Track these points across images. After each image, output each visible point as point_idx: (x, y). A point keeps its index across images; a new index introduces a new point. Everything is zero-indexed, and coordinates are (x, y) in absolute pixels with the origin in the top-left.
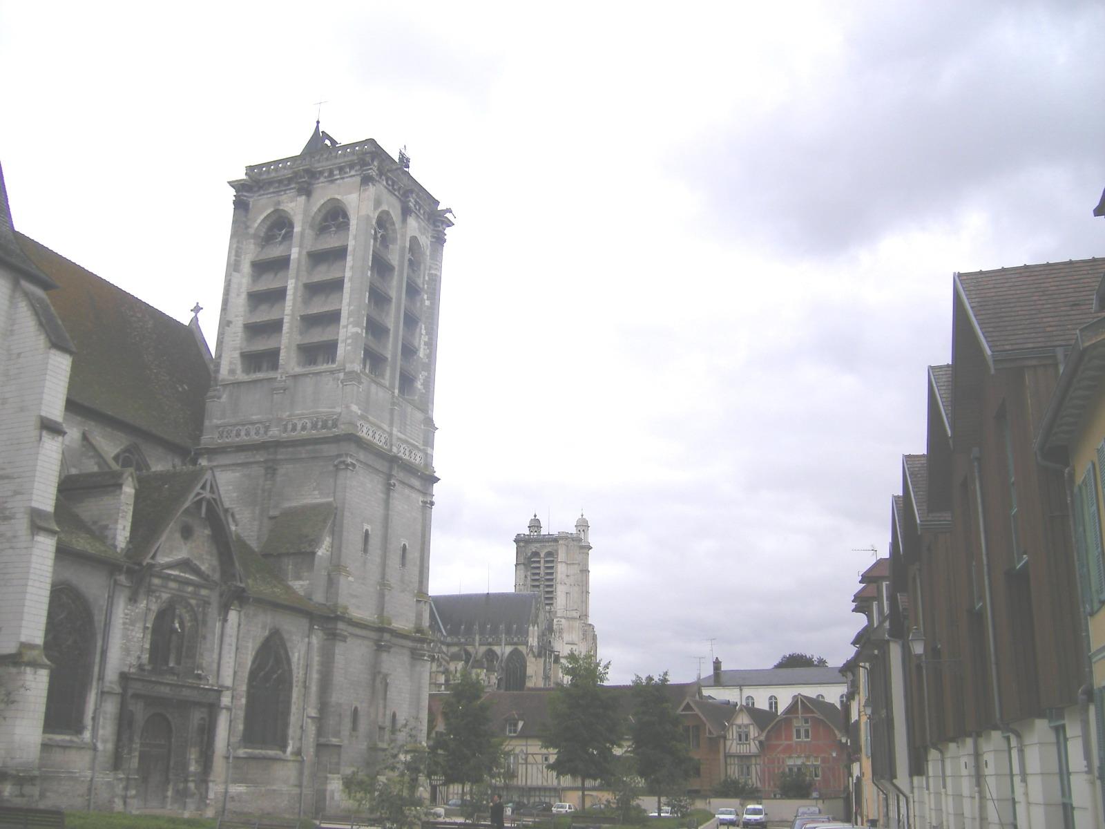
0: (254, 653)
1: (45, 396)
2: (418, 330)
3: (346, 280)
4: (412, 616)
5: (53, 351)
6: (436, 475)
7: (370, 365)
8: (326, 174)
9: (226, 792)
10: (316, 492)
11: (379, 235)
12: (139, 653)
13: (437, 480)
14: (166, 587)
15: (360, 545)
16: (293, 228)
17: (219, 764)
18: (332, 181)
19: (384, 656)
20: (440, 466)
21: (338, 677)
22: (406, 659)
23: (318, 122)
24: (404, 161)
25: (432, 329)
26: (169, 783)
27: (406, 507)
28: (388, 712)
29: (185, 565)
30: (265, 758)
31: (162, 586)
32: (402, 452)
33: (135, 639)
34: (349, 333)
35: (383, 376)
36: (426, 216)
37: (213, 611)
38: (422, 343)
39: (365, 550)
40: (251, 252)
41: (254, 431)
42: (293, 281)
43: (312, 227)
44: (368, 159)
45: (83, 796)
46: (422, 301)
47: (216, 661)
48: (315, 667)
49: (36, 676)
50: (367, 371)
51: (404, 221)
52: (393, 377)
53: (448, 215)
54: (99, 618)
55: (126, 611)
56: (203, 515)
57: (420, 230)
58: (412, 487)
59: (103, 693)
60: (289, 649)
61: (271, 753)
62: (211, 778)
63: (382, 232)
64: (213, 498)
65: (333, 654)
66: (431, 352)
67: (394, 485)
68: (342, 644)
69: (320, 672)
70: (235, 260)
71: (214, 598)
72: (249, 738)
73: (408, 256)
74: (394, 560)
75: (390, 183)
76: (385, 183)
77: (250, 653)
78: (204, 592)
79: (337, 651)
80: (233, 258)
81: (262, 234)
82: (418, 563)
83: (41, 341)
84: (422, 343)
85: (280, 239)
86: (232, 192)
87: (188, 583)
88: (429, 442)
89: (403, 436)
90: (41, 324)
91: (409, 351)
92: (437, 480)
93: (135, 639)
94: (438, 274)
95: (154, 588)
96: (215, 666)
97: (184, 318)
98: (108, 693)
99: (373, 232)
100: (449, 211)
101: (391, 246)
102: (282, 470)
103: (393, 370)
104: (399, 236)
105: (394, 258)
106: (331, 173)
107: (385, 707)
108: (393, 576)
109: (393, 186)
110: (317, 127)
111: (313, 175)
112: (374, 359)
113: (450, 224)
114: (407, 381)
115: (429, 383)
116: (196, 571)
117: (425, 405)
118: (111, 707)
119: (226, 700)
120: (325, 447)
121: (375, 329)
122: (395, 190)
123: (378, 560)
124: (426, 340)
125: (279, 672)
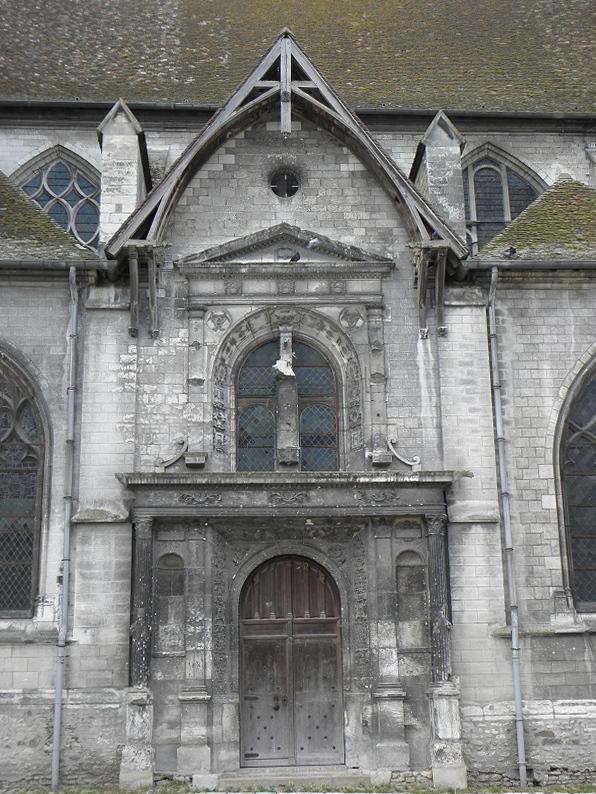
33: (166, 409)
45: (33, 743)
54: (49, 383)
55: (124, 358)
59: (73, 526)
64: (308, 91)
77: (547, 392)
93: (166, 409)
95: (200, 301)
96: (431, 433)
98: (76, 524)
118: (105, 553)
119: (474, 502)
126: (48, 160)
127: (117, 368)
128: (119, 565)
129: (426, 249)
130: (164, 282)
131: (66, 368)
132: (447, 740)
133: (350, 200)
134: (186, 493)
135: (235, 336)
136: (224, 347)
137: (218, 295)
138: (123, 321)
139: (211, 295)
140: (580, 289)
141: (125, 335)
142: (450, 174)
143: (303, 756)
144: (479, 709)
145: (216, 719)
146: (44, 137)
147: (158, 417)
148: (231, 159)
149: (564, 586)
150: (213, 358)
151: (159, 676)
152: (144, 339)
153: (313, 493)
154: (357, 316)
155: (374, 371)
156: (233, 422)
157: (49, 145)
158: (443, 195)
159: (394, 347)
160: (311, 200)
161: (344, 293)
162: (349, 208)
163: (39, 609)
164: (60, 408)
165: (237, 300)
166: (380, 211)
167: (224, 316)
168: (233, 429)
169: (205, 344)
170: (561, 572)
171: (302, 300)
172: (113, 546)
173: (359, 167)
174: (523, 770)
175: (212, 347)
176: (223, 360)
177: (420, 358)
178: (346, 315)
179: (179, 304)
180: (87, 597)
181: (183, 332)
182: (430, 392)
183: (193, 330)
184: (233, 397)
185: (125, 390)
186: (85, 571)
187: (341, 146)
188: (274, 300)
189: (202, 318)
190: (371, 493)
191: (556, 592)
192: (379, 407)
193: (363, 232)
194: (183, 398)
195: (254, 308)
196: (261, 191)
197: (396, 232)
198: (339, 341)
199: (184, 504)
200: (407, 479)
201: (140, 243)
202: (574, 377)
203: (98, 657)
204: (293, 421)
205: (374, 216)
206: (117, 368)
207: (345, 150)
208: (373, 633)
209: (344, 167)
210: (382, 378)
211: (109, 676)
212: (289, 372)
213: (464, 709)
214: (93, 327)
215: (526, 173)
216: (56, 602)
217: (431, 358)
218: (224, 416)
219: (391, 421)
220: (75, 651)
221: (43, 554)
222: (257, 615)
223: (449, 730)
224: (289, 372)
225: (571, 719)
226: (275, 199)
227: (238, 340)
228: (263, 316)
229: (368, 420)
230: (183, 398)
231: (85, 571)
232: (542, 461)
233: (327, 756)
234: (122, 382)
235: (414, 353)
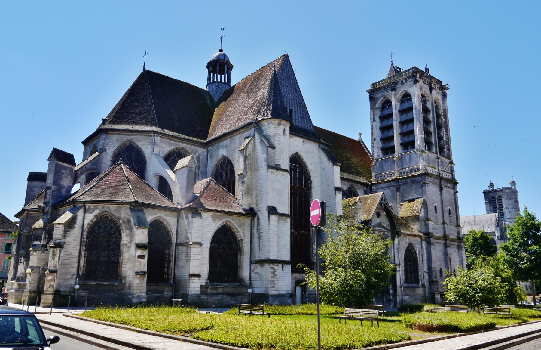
1: (335, 181)
2: (442, 131)
3: (414, 119)
4: (456, 234)
6: (457, 182)
7: (427, 146)
8: (400, 82)
9: (402, 299)
10: (416, 194)
11: (423, 100)
13: (458, 183)
15: (434, 211)
16: (392, 103)
17: (399, 289)
18: (403, 84)
19: (448, 249)
20: (458, 178)
21: (434, 258)
22: (456, 249)
23: (392, 61)
24: (427, 70)
25: (447, 129)
26: (384, 297)
27: (448, 195)
28: (452, 269)
29: (380, 225)
30: (413, 287)
32: (444, 175)
34: (419, 137)
35: (432, 149)
36: (439, 88)
38: (444, 135)
39: (436, 213)
40: (378, 113)
41: (390, 175)
42: (395, 122)
43: (398, 102)
44: (415, 74)
46: (442, 119)
47: (393, 256)
48: (425, 255)
50: (427, 149)
51: (431, 92)
52: (436, 150)
53: (447, 86)
56: (383, 209)
57: (437, 94)
58: (449, 187)
61: (414, 285)
62: (397, 295)
63: (424, 98)
65: (431, 250)
66: (448, 137)
67: (443, 188)
68: (433, 246)
69: (427, 257)
70: (373, 117)
72: (407, 281)
73: (434, 104)
74: (446, 214)
75: (424, 80)
76: (422, 81)
78: (386, 233)
79: (432, 249)
80: (372, 117)
81: (381, 107)
82: (455, 214)
83: (330, 164)
84: (444, 135)
85: (387, 107)
86: (368, 94)
87: (381, 231)
88: (452, 170)
89: (443, 170)
90: (329, 158)
91: (440, 138)
92: (458, 183)
94: (446, 108)
96: (393, 258)
97: (356, 138)
99: (421, 100)
100: (447, 85)
101: (428, 103)
102: (402, 188)
103: (436, 147)
104: (430, 98)
105: (429, 106)
106: (402, 82)
107: (451, 267)
108: (447, 220)
109: (425, 81)
110: (392, 64)
111: (396, 83)
112: (428, 144)
113: (448, 89)
114: (441, 149)
115: (449, 149)
116: (383, 227)
117: (449, 157)
120: (416, 178)
121: (427, 133)
122: (426, 82)
123: (441, 215)
124: (446, 133)
125: (413, 257)
161: (385, 234)
226: (377, 218)
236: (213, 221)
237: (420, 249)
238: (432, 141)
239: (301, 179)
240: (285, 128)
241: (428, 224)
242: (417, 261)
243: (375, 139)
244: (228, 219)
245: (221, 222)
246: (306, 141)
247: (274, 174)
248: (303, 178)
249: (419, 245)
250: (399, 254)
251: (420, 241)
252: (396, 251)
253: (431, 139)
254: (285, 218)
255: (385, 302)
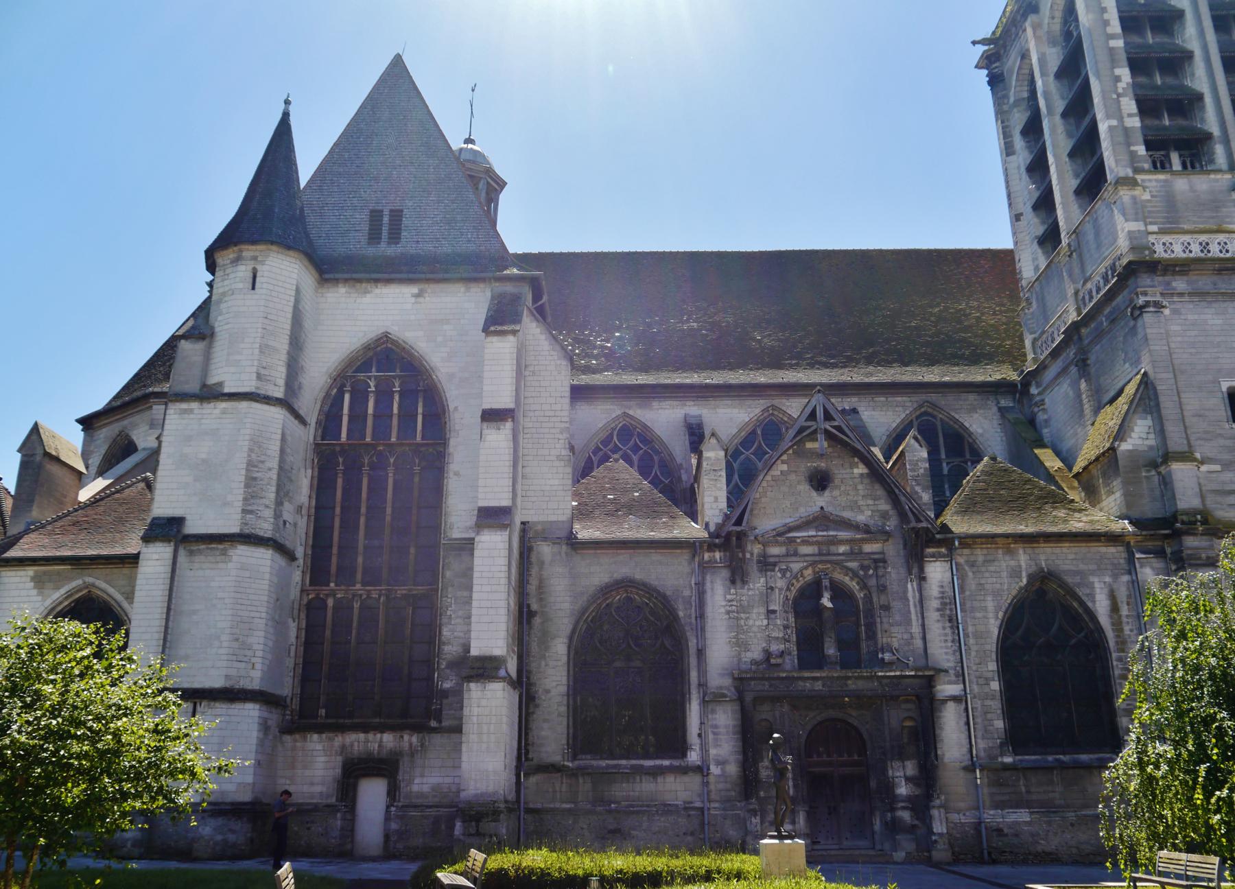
0: (1001, 615)
5: (490, 339)
10: (1127, 365)
12: (764, 645)
14: (796, 554)
31: (787, 555)
35: (1212, 161)
37: (894, 573)
45: (692, 834)
49: (485, 692)
55: (729, 597)
59: (704, 703)
60: (1084, 598)
64: (834, 427)
71: (893, 550)
77: (991, 615)
95: (772, 560)
96: (918, 643)
118: (725, 718)
126: (617, 423)
127: (724, 603)
128: (734, 726)
129: (913, 528)
130: (749, 548)
131: (693, 604)
132: (939, 834)
133: (861, 492)
134: (773, 682)
135: (794, 581)
136: (788, 589)
137: (783, 556)
138: (725, 573)
139: (778, 556)
140: (1010, 547)
141: (728, 583)
142: (922, 471)
143: (846, 843)
144: (956, 815)
145: (797, 820)
146: (615, 407)
147: (751, 634)
148: (785, 467)
149: (1006, 739)
150: (782, 596)
151: (762, 794)
152: (739, 583)
153: (850, 682)
154: (868, 568)
155: (882, 603)
156: (794, 635)
157: (619, 412)
158: (918, 485)
159: (894, 587)
160: (836, 493)
161: (861, 553)
162: (861, 498)
163: (689, 753)
164: (692, 629)
165: (794, 559)
166: (880, 499)
167: (787, 569)
168: (795, 640)
169: (776, 587)
170: (1003, 730)
171: (834, 558)
172: (730, 715)
173: (865, 471)
174: (986, 852)
175: (781, 590)
176: (787, 596)
177: (910, 594)
178: (862, 567)
179: (759, 562)
180: (717, 746)
181: (762, 580)
182: (917, 616)
183: (768, 578)
184: (793, 619)
185: (730, 618)
186: (715, 730)
187: (853, 457)
188: (817, 558)
189: (774, 571)
190: (885, 681)
191: (1001, 743)
192: (886, 626)
193: (870, 513)
194: (765, 622)
195: (805, 564)
196: (804, 487)
197: (891, 512)
198: (858, 583)
199: (772, 689)
200: (907, 673)
201: (738, 529)
202: (1007, 605)
203: (726, 782)
204: (833, 636)
205: (876, 502)
206: (724, 603)
207: (856, 460)
208: (889, 768)
209: (856, 471)
210: (887, 608)
211: (733, 794)
212: (830, 605)
213: (948, 815)
214: (708, 578)
215: (955, 423)
216: (698, 749)
217: (917, 594)
218: (789, 632)
219: (893, 635)
220: (711, 779)
221: (688, 719)
222: (815, 756)
223: (940, 828)
224: (830, 605)
225: (1013, 822)
226: (814, 494)
227: (795, 583)
228: (810, 568)
229: (879, 635)
230: (765, 622)
231: (715, 730)
232: (989, 659)
233: (861, 843)
234: (728, 612)
235: (905, 591)
236: (35, 592)
237: (1122, 593)
238: (1206, 128)
239: (408, 418)
240: (259, 267)
241: (1170, 473)
242: (1106, 649)
243: (1021, 214)
244: (90, 580)
245: (63, 591)
246: (431, 287)
247: (192, 416)
248: (420, 410)
249: (1115, 577)
250: (955, 626)
251: (1124, 555)
252: (933, 616)
253: (1203, 120)
254: (221, 547)
255: (877, 837)
